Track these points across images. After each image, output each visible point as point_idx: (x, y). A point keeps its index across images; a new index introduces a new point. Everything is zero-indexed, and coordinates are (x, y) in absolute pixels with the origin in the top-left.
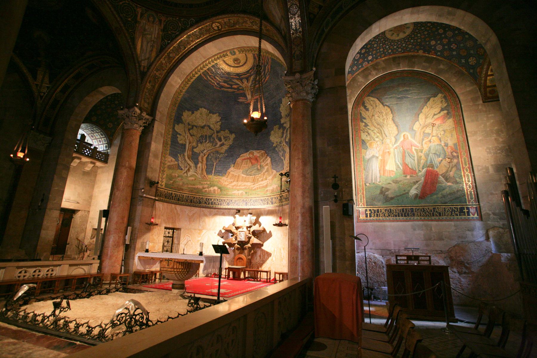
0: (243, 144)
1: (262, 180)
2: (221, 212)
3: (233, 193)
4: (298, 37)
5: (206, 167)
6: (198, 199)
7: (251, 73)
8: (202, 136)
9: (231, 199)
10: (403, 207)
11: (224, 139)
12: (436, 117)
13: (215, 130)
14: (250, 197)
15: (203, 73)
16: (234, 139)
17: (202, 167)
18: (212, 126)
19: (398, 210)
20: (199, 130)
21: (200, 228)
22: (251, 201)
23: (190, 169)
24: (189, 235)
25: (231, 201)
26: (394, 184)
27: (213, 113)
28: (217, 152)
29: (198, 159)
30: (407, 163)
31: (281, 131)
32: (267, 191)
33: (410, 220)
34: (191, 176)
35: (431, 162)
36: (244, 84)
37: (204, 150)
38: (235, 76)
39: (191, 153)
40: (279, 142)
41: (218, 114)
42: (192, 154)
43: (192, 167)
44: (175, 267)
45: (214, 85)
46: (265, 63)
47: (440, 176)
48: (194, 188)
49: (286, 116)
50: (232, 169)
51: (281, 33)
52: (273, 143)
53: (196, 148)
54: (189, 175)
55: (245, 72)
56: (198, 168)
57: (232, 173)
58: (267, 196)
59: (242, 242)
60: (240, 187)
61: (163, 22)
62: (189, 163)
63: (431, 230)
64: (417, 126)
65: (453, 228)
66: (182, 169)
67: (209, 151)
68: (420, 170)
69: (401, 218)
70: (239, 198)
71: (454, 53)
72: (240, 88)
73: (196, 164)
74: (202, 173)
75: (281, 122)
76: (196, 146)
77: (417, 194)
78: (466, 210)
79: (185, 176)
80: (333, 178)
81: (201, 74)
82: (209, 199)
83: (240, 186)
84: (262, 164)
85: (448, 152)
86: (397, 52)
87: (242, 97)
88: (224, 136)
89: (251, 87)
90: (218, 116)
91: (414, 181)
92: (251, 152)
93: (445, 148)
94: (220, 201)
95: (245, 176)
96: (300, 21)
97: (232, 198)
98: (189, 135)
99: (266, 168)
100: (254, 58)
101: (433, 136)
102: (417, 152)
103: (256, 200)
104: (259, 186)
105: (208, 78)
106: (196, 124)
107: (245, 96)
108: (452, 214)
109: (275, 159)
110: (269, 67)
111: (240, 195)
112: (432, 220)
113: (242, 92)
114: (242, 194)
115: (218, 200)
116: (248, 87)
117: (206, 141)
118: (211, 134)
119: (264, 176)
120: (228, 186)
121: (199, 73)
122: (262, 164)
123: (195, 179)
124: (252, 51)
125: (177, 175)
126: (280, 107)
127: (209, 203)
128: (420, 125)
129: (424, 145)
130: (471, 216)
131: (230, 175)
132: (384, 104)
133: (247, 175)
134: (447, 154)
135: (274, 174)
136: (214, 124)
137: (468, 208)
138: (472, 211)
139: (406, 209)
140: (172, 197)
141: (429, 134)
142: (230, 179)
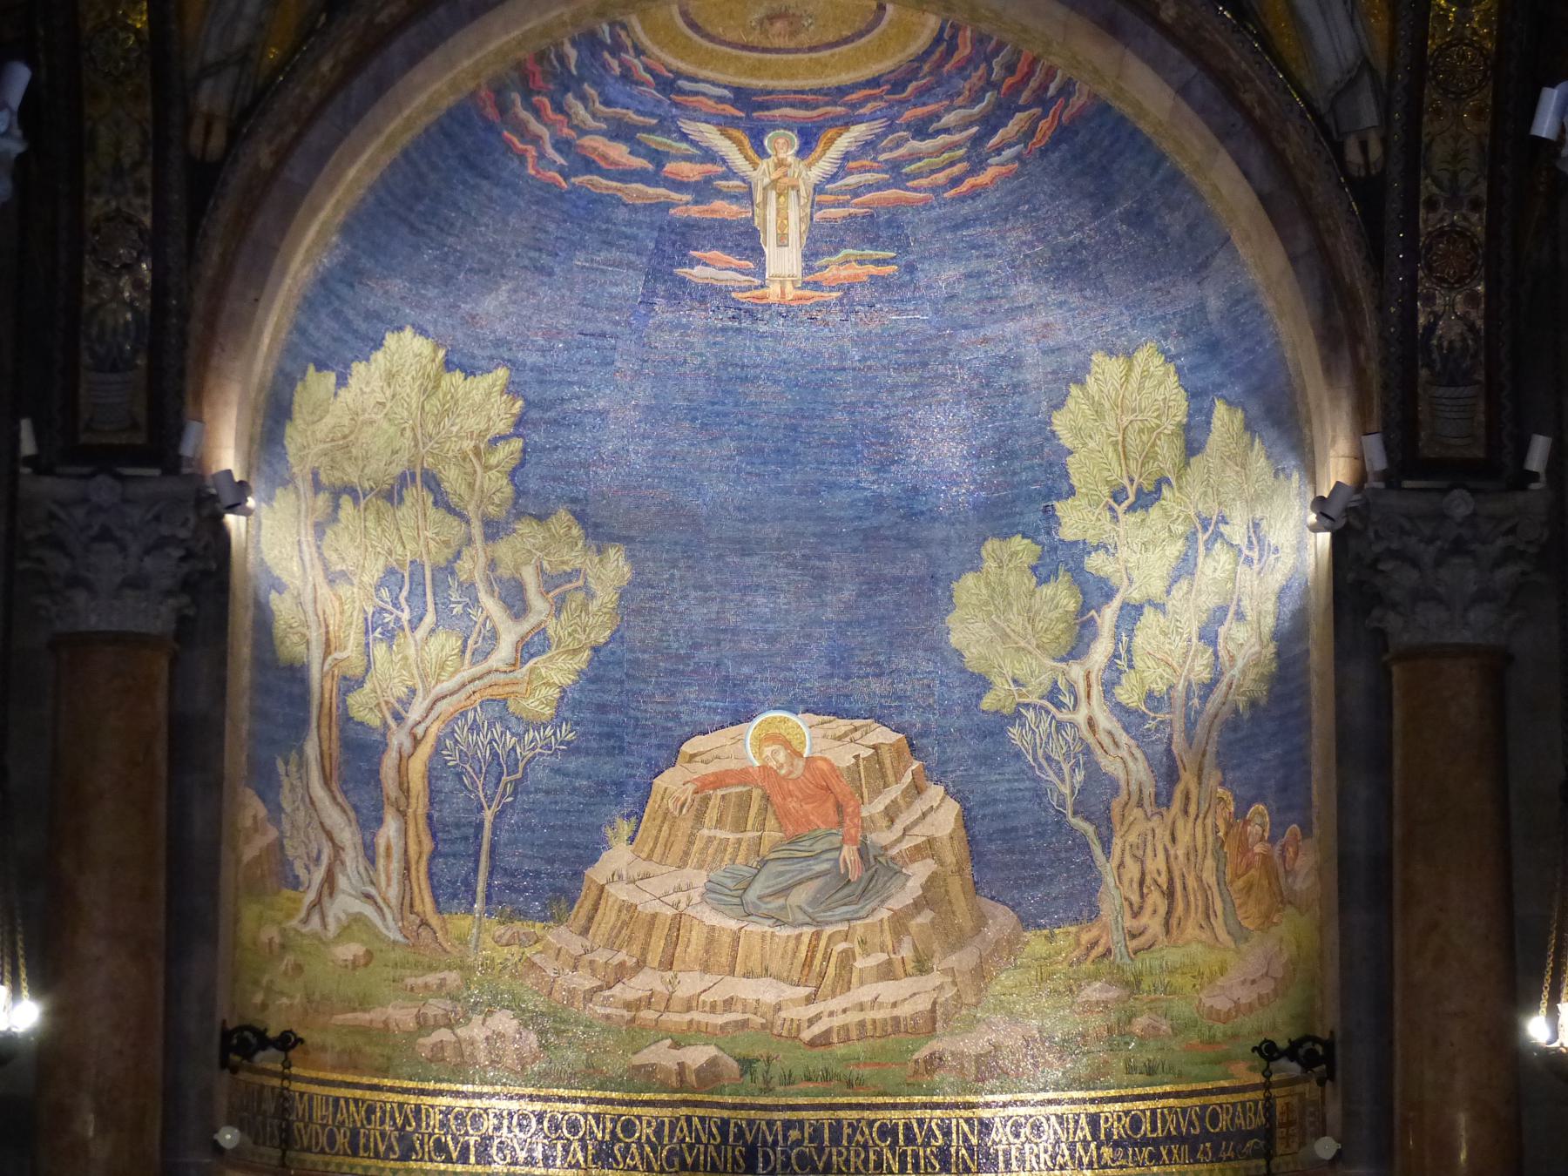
0: (696, 646)
1: (887, 972)
3: (637, 1060)
4: (1462, 234)
5: (428, 845)
7: (854, 106)
13: (471, 510)
14: (782, 1101)
18: (452, 478)
22: (794, 1134)
23: (337, 869)
25: (629, 1128)
27: (469, 372)
28: (500, 712)
29: (374, 775)
31: (1061, 596)
32: (933, 1062)
36: (764, 165)
37: (413, 691)
38: (721, 100)
41: (502, 374)
43: (352, 857)
45: (532, 151)
46: (1016, 90)
48: (364, 1031)
49: (1118, 495)
50: (617, 857)
52: (982, 683)
54: (333, 927)
56: (381, 862)
57: (620, 893)
60: (696, 1016)
62: (328, 823)
66: (296, 884)
67: (442, 706)
70: (685, 1103)
73: (369, 822)
74: (407, 904)
76: (359, 671)
79: (315, 935)
81: (473, 94)
82: (460, 1117)
83: (689, 1009)
87: (724, 248)
88: (540, 570)
89: (818, 189)
92: (769, 722)
95: (733, 924)
96: (1487, 141)
97: (631, 1103)
98: (320, 579)
100: (938, 40)
104: (853, 1017)
105: (503, 109)
106: (352, 475)
107: (756, 252)
109: (1005, 816)
110: (1043, 124)
113: (725, 209)
114: (710, 1076)
116: (795, 187)
118: (448, 553)
119: (898, 941)
121: (471, 85)
122: (882, 837)
123: (369, 954)
125: (277, 940)
126: (1059, 406)
127: (466, 1147)
131: (607, 918)
135: (990, 933)
142: (610, 945)
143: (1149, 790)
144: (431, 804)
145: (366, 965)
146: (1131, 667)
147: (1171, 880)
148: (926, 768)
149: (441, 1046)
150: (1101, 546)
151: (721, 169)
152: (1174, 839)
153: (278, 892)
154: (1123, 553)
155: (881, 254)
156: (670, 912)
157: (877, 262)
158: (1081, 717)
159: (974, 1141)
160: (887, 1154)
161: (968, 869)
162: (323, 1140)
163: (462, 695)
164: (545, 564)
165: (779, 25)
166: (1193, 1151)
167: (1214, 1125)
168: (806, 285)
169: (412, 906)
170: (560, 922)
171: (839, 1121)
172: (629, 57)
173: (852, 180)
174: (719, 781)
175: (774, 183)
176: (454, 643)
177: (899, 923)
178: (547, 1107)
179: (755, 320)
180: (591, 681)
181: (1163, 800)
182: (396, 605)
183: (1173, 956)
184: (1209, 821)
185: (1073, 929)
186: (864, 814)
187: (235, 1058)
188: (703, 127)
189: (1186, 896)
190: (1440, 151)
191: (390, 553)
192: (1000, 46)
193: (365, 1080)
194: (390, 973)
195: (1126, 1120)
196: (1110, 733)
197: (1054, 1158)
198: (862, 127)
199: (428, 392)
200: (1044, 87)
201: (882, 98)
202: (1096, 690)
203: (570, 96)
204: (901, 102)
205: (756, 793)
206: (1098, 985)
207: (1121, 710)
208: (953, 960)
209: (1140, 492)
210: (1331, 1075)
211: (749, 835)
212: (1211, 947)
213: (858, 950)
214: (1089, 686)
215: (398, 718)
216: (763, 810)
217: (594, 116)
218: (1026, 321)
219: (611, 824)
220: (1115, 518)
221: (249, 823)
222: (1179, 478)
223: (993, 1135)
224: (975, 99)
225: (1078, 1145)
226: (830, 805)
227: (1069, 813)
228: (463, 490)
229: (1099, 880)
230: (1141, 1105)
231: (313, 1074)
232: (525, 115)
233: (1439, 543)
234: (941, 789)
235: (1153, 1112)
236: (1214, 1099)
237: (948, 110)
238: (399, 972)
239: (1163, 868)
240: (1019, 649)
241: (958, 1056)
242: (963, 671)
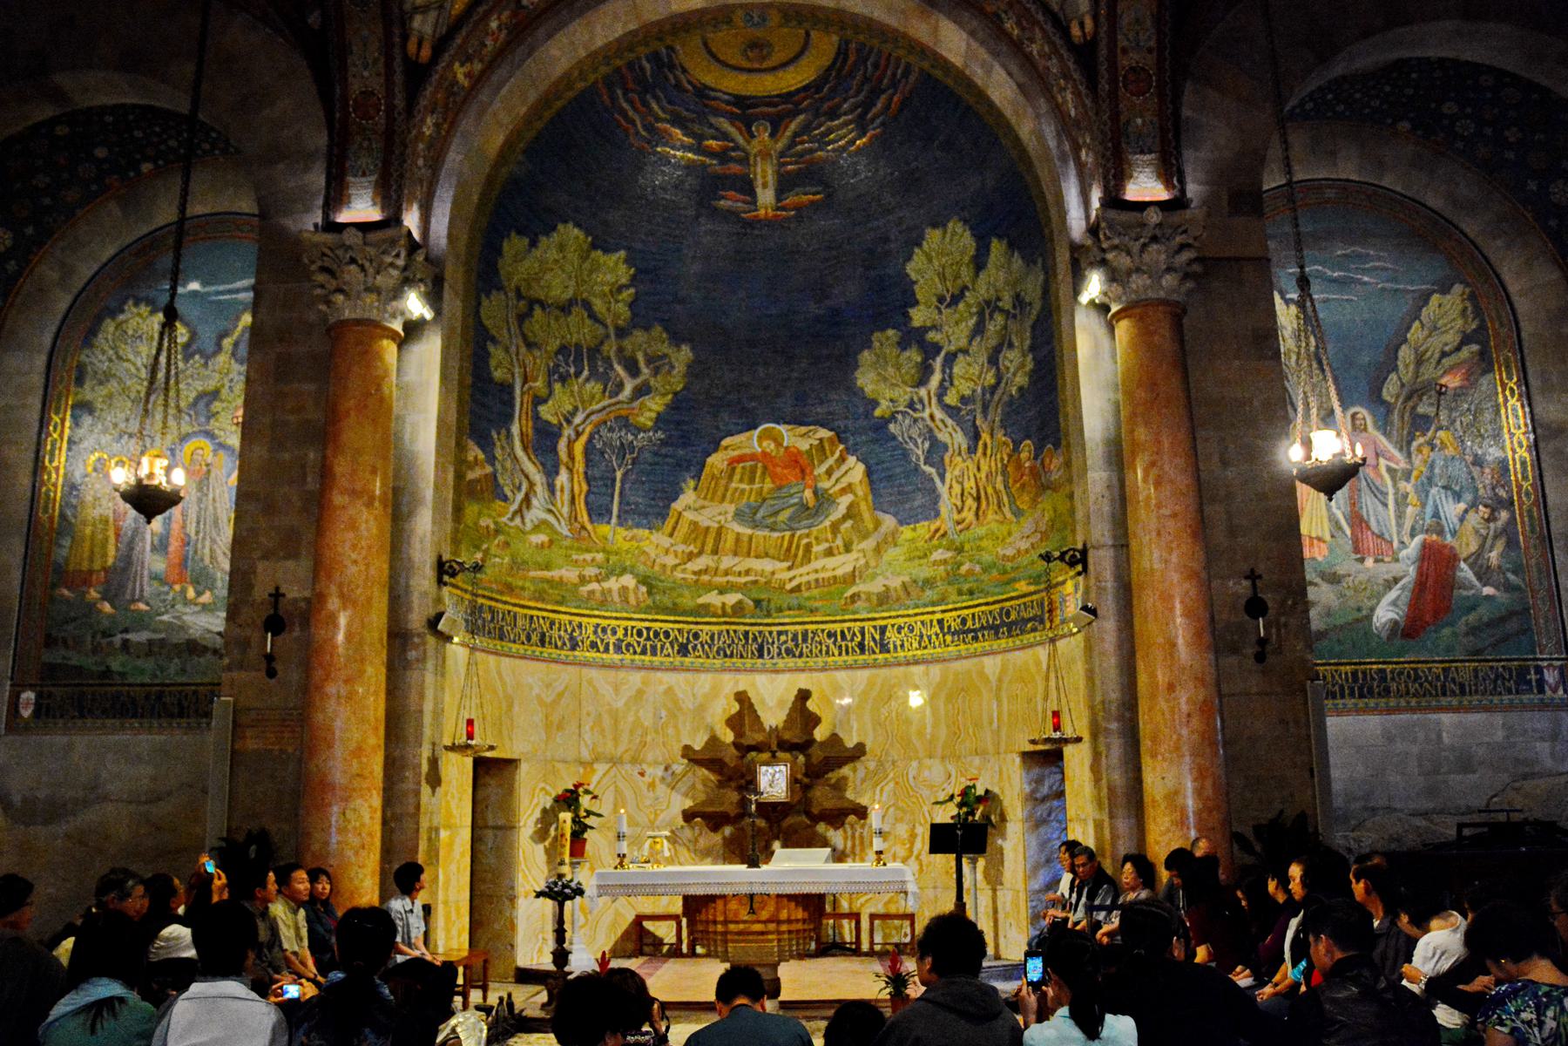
1: (829, 553)
2: (661, 683)
3: (701, 601)
5: (585, 487)
6: (566, 631)
8: (563, 350)
9: (695, 628)
10: (1355, 664)
11: (647, 366)
12: (1446, 362)
13: (609, 321)
14: (777, 621)
15: (606, 78)
16: (689, 367)
17: (572, 490)
18: (598, 305)
19: (1340, 675)
20: (552, 322)
21: (586, 755)
22: (783, 638)
23: (531, 495)
24: (548, 788)
25: (696, 636)
26: (1325, 587)
27: (606, 251)
28: (624, 423)
29: (554, 450)
30: (1365, 517)
32: (854, 598)
33: (1375, 710)
34: (537, 528)
35: (1436, 515)
36: (755, 142)
37: (576, 409)
38: (728, 103)
39: (530, 424)
42: (537, 430)
44: (784, 915)
46: (880, 80)
47: (1463, 565)
48: (548, 581)
49: (941, 299)
50: (688, 498)
51: (1065, 32)
52: (875, 403)
53: (545, 401)
54: (529, 526)
55: (778, 96)
56: (558, 493)
58: (855, 620)
59: (774, 806)
60: (730, 578)
63: (1439, 736)
65: (1499, 735)
66: (505, 499)
67: (593, 418)
68: (1406, 539)
69: (1350, 702)
70: (726, 623)
71: (1511, 155)
72: (733, 154)
73: (551, 472)
74: (573, 517)
75: (911, 319)
76: (544, 392)
77: (1396, 623)
79: (518, 527)
80: (1246, 578)
81: (596, 82)
82: (604, 630)
83: (726, 573)
85: (1484, 487)
86: (1329, 114)
88: (646, 354)
89: (782, 154)
90: (626, 261)
91: (1386, 577)
92: (765, 429)
93: (1476, 471)
94: (648, 638)
95: (749, 531)
97: (697, 623)
98: (521, 344)
100: (838, 53)
101: (1441, 428)
102: (1394, 479)
103: (805, 634)
104: (812, 577)
105: (613, 99)
107: (751, 192)
108: (1495, 688)
111: (729, 610)
112: (1441, 709)
113: (735, 168)
114: (738, 609)
115: (640, 634)
116: (770, 155)
117: (581, 372)
121: (592, 78)
122: (825, 484)
123: (551, 542)
124: (842, 28)
125: (492, 526)
126: (909, 258)
127: (608, 644)
128: (1403, 385)
129: (1413, 456)
130: (1549, 693)
131: (683, 529)
132: (1288, 296)
133: (756, 525)
134: (1481, 492)
135: (883, 529)
136: (605, 295)
137: (1539, 670)
139: (1364, 673)
140: (484, 626)
141: (1426, 417)
142: (685, 542)
143: (964, 447)
144: (587, 466)
145: (549, 547)
146: (952, 384)
147: (978, 491)
148: (847, 449)
149: (592, 592)
150: (934, 327)
151: (731, 144)
152: (979, 469)
153: (493, 501)
154: (946, 328)
155: (814, 189)
156: (716, 525)
157: (814, 194)
158: (926, 414)
159: (877, 637)
160: (832, 646)
161: (870, 498)
162: (523, 638)
163: (604, 412)
164: (649, 351)
165: (757, 51)
166: (997, 633)
167: (1008, 617)
168: (778, 209)
169: (576, 518)
170: (658, 530)
171: (806, 631)
172: (678, 73)
173: (799, 147)
174: (741, 459)
175: (760, 151)
176: (599, 387)
177: (835, 528)
178: (656, 626)
179: (753, 228)
180: (673, 409)
181: (972, 450)
182: (567, 364)
183: (981, 531)
184: (999, 456)
185: (926, 523)
186: (816, 473)
187: (446, 578)
188: (722, 120)
189: (987, 498)
191: (563, 337)
192: (871, 49)
193: (549, 607)
194: (563, 552)
195: (959, 621)
196: (942, 421)
197: (920, 643)
198: (802, 117)
199: (584, 258)
200: (894, 75)
201: (812, 97)
202: (934, 400)
203: (648, 96)
204: (821, 99)
205: (760, 465)
206: (940, 551)
207: (950, 411)
208: (864, 545)
209: (953, 296)
210: (1085, 569)
211: (757, 486)
212: (1002, 523)
213: (814, 542)
214: (930, 398)
215: (569, 422)
216: (763, 474)
217: (662, 109)
218: (891, 217)
219: (685, 481)
220: (940, 312)
221: (471, 458)
222: (973, 284)
223: (887, 634)
224: (858, 92)
225: (934, 637)
226: (798, 470)
227: (922, 463)
228: (604, 310)
229: (939, 496)
230: (966, 612)
231: (517, 601)
232: (625, 105)
233: (1142, 240)
234: (854, 458)
235: (973, 615)
236: (1008, 604)
237: (845, 100)
238: (569, 552)
239: (973, 484)
240: (892, 384)
241: (869, 594)
242: (864, 398)
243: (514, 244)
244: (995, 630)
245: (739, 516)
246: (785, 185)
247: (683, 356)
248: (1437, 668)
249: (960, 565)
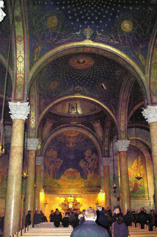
1: (76, 182)
8: (51, 162)
18: (54, 156)
21: (52, 203)
32: (79, 187)
40: (84, 167)
47: (139, 185)
49: (88, 157)
50: (62, 176)
52: (81, 167)
61: (54, 123)
64: (132, 167)
78: (145, 196)
83: (66, 184)
84: (76, 175)
99: (78, 177)
112: (136, 200)
120: (61, 184)
122: (76, 175)
130: (146, 198)
138: (147, 196)
143: (90, 173)
190: (106, 140)
243: (47, 151)
244: (92, 191)
245: (67, 178)
246: (73, 144)
247: (62, 161)
248: (136, 195)
249: (89, 184)
